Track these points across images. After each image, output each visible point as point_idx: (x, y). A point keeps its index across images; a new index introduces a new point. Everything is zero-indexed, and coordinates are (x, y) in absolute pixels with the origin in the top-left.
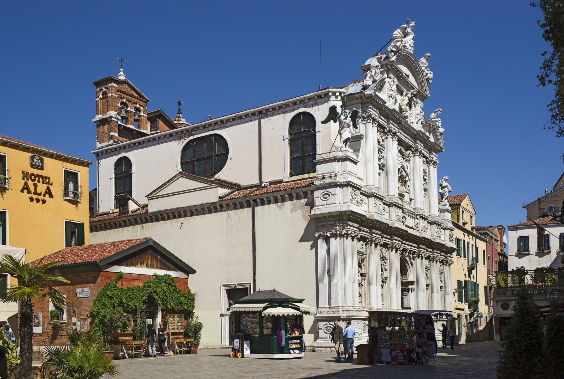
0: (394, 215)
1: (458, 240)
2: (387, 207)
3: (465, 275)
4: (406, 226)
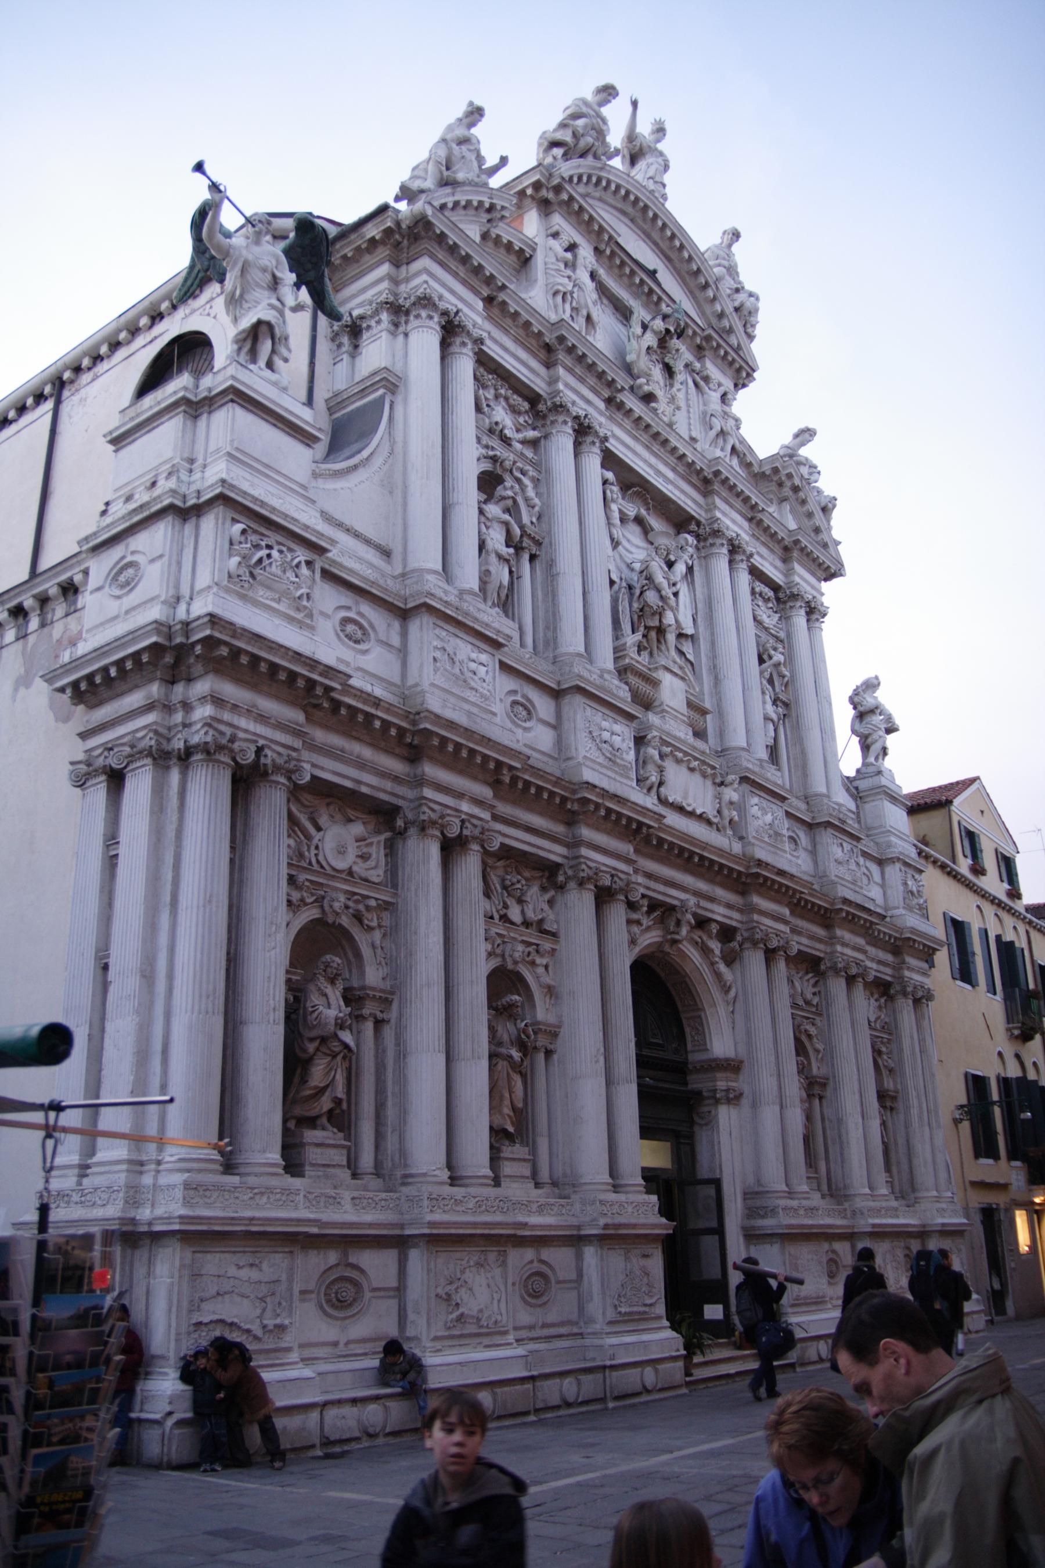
1: (958, 928)
2: (543, 705)
3: (1000, 1054)
4: (663, 801)
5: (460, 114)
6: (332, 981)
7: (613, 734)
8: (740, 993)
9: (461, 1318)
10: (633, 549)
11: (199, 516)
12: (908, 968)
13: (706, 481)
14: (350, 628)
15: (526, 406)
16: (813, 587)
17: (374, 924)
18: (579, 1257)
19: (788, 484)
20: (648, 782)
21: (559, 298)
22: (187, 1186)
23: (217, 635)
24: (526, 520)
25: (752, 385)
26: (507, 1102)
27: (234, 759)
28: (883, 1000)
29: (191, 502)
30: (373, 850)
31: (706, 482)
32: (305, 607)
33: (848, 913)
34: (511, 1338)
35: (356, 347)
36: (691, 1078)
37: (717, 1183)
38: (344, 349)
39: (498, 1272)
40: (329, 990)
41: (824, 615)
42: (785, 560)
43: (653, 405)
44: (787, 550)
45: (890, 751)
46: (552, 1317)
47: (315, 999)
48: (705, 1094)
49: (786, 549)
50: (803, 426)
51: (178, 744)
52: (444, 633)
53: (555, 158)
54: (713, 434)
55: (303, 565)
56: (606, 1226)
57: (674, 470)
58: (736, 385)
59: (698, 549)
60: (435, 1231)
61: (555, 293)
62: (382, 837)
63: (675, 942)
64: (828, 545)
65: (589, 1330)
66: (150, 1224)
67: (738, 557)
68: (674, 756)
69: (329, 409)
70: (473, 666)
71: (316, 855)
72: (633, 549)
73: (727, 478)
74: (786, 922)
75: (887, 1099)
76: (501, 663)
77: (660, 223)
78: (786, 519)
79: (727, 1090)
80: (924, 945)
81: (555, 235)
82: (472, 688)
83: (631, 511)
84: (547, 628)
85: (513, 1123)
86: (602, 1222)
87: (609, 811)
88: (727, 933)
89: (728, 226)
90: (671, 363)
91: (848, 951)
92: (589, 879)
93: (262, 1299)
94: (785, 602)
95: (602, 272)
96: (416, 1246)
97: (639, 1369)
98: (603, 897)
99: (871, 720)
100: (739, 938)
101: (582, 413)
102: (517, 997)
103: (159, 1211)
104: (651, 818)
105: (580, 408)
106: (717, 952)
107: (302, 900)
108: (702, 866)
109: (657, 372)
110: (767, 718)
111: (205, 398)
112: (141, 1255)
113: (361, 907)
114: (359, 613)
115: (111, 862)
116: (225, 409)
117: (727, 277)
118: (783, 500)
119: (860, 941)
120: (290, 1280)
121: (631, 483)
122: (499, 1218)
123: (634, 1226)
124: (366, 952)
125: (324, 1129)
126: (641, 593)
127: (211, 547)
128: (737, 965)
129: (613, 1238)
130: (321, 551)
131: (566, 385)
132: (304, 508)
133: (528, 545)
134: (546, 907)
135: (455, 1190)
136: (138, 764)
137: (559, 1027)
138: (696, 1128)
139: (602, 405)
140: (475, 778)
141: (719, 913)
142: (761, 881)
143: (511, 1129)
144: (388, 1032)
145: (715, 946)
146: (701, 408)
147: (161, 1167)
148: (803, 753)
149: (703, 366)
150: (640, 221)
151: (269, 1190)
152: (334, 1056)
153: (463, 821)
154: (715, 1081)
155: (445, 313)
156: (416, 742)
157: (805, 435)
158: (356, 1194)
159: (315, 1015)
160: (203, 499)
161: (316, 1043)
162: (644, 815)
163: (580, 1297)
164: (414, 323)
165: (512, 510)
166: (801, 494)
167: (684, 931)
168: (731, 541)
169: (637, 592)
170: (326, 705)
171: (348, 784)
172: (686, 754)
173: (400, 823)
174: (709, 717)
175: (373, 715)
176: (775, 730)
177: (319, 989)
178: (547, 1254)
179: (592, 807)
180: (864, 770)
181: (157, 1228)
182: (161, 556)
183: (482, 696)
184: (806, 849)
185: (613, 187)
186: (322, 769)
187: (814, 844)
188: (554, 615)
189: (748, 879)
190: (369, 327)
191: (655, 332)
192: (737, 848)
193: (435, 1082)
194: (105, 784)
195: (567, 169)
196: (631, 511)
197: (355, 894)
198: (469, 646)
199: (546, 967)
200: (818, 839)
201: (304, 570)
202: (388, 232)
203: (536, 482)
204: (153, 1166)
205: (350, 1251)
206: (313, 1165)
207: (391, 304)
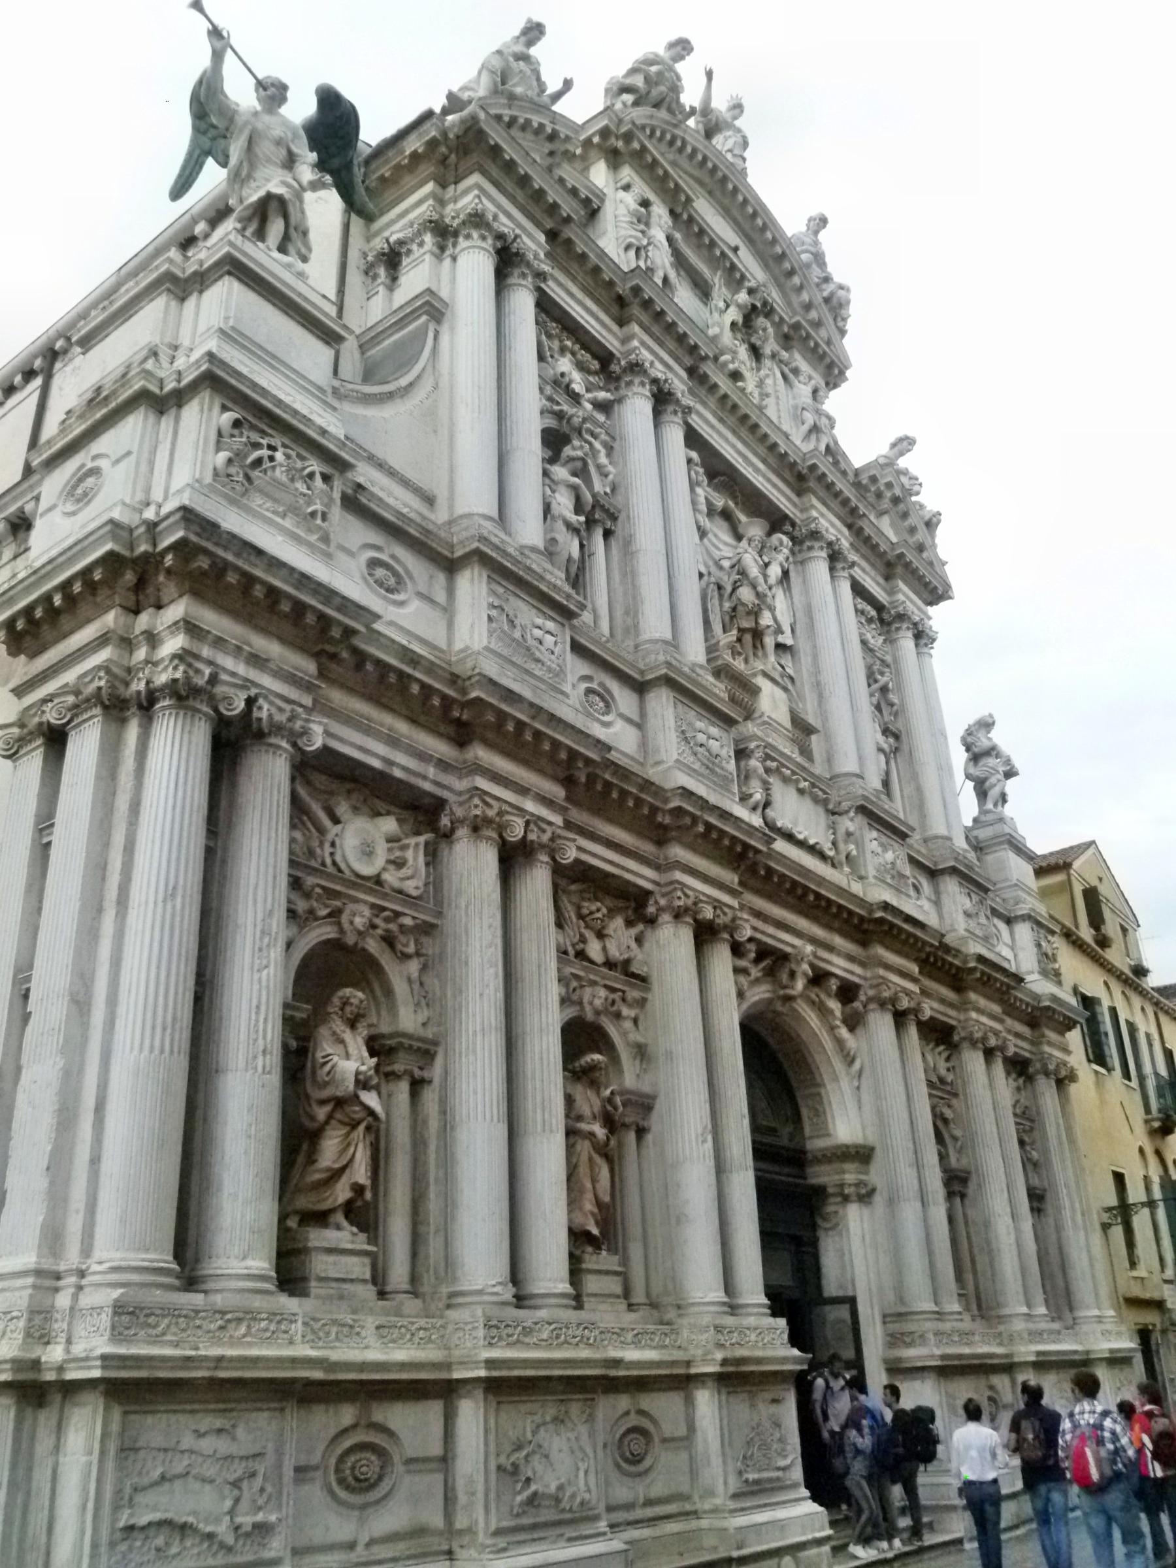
0: (673, 736)
1: (1088, 1002)
2: (624, 699)
3: (1141, 1151)
5: (517, 33)
6: (352, 1024)
7: (709, 737)
8: (867, 1064)
9: (533, 1501)
10: (721, 546)
11: (180, 406)
12: (1050, 1044)
13: (801, 477)
14: (380, 572)
15: (595, 365)
16: (919, 609)
17: (411, 949)
18: (689, 1402)
19: (889, 494)
20: (753, 800)
21: (632, 253)
22: (119, 1308)
23: (194, 538)
24: (598, 486)
25: (844, 386)
26: (589, 1196)
27: (216, 710)
28: (1021, 1081)
29: (170, 386)
30: (409, 854)
31: (801, 478)
32: (320, 528)
33: (983, 973)
34: (602, 1525)
35: (394, 279)
36: (811, 1170)
37: (852, 1301)
38: (379, 281)
39: (583, 1429)
40: (348, 1036)
41: (934, 640)
42: (887, 578)
43: (740, 384)
44: (892, 567)
45: (1009, 798)
46: (658, 1489)
47: (326, 1047)
48: (830, 1190)
49: (889, 565)
50: (900, 434)
51: (139, 686)
52: (501, 590)
53: (624, 104)
54: (806, 427)
55: (318, 478)
56: (725, 1362)
57: (764, 461)
58: (827, 384)
59: (792, 552)
60: (495, 1374)
61: (628, 248)
62: (422, 839)
63: (789, 999)
64: (935, 564)
65: (707, 1507)
66: (61, 1369)
67: (839, 565)
68: (780, 773)
69: (361, 346)
70: (538, 633)
71: (332, 854)
72: (721, 546)
73: (824, 475)
74: (914, 980)
75: (1038, 1199)
76: (572, 639)
77: (740, 198)
78: (887, 529)
79: (857, 1185)
80: (1065, 1016)
81: (627, 188)
82: (538, 661)
83: (720, 502)
84: (627, 613)
85: (597, 1223)
86: (719, 1356)
87: (709, 827)
88: (847, 992)
89: (814, 212)
90: (758, 343)
91: (984, 1019)
92: (687, 910)
93: (236, 1484)
94: (889, 624)
95: (678, 236)
96: (469, 1395)
97: (776, 1560)
98: (705, 934)
99: (987, 763)
100: (863, 998)
101: (660, 375)
102: (597, 1057)
103: (78, 1349)
105: (658, 371)
106: (838, 1014)
107: (311, 912)
108: (818, 907)
109: (743, 352)
110: (880, 750)
111: (195, 273)
112: (46, 1419)
113: (393, 927)
114: (393, 557)
115: (42, 850)
116: (220, 283)
117: (814, 266)
118: (881, 514)
119: (996, 1009)
120: (279, 1453)
121: (718, 471)
122: (584, 1353)
123: (759, 1361)
124: (400, 987)
125: (338, 1227)
126: (734, 590)
127: (193, 436)
128: (860, 1031)
129: (737, 1379)
130: (343, 466)
131: (643, 343)
132: (322, 412)
133: (600, 517)
134: (633, 945)
135: (521, 1313)
136: (85, 716)
137: (654, 1097)
138: (821, 1234)
139: (684, 374)
140: (541, 772)
141: (839, 966)
142: (886, 928)
143: (595, 1231)
144: (430, 1096)
145: (834, 1005)
146: (791, 402)
147: (84, 1282)
148: (919, 790)
149: (791, 356)
150: (718, 193)
151: (250, 1315)
152: (354, 1126)
153: (527, 823)
154: (844, 1172)
155: (500, 237)
156: (465, 717)
157: (904, 444)
158: (381, 1320)
159: (327, 1068)
160: (184, 382)
161: (327, 1108)
162: (751, 835)
163: (691, 1458)
164: (462, 243)
165: (582, 471)
166: (902, 506)
167: (800, 984)
168: (830, 544)
169: (729, 589)
170: (345, 654)
171: (376, 764)
172: (794, 773)
173: (445, 821)
174: (814, 738)
175: (409, 676)
176: (887, 763)
177: (334, 1033)
178: (647, 1401)
179: (688, 821)
180: (983, 818)
181: (71, 1375)
182: (129, 453)
183: (550, 670)
184: (929, 899)
185: (689, 149)
186: (341, 740)
187: (937, 893)
188: (634, 598)
189: (871, 928)
190: (409, 252)
191: (739, 306)
192: (856, 888)
193: (491, 1156)
194: (42, 749)
195: (641, 115)
196: (720, 502)
197: (384, 909)
198: (534, 611)
199: (635, 1021)
200: (942, 887)
201: (318, 482)
202: (432, 144)
203: (610, 449)
204: (73, 1280)
205: (374, 1405)
206: (321, 1279)
207: (435, 222)
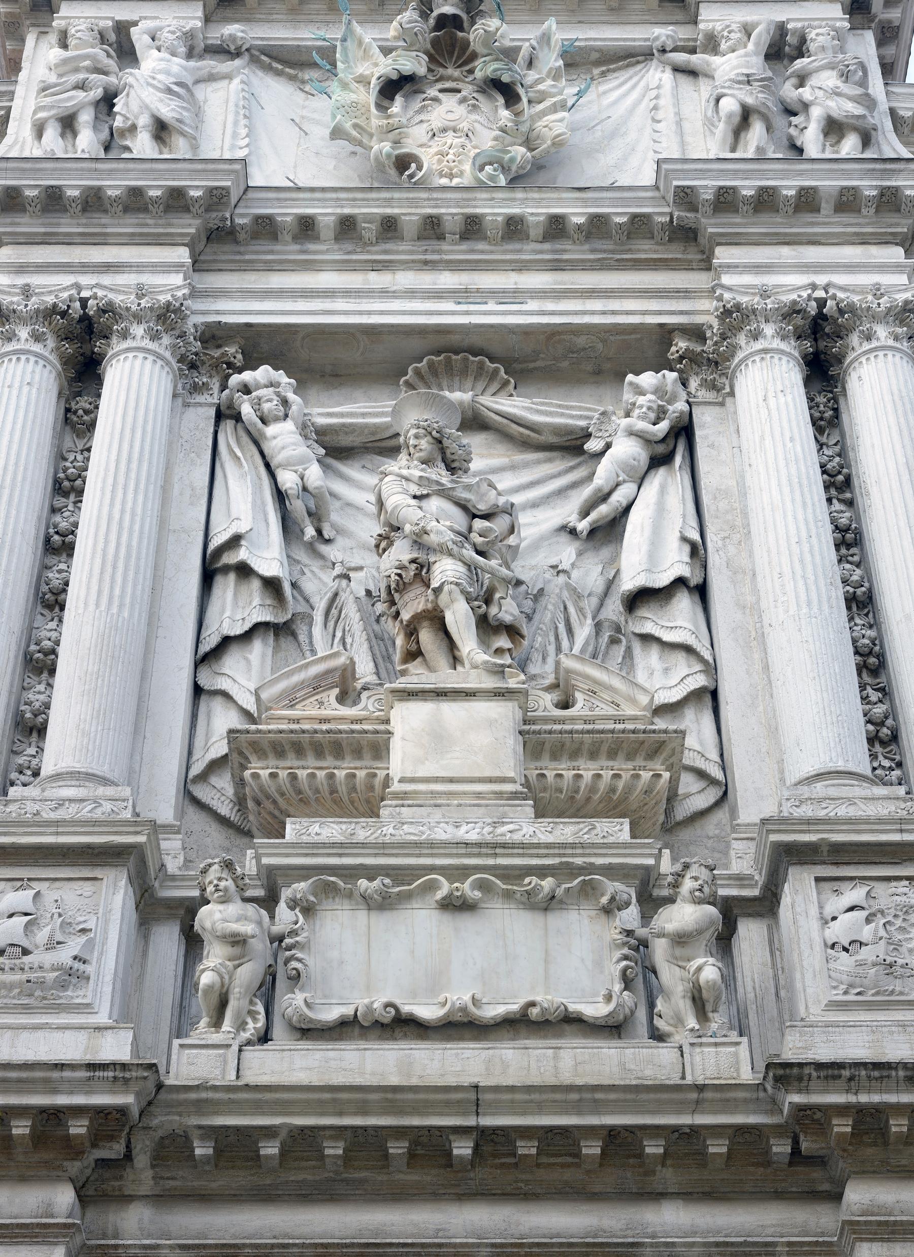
57: (557, 266)
104: (86, 1085)
162: (51, 1088)
